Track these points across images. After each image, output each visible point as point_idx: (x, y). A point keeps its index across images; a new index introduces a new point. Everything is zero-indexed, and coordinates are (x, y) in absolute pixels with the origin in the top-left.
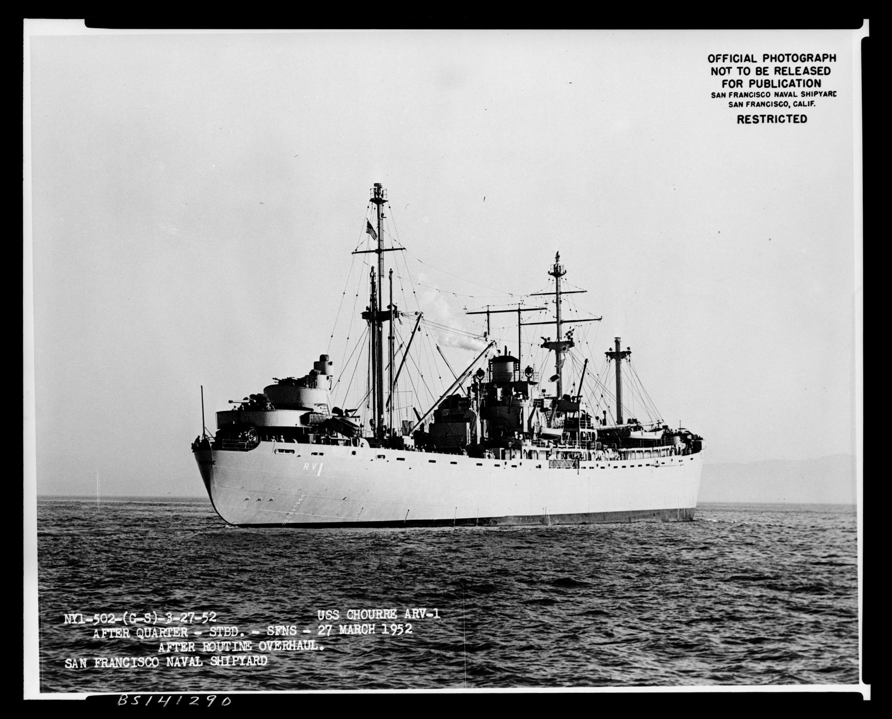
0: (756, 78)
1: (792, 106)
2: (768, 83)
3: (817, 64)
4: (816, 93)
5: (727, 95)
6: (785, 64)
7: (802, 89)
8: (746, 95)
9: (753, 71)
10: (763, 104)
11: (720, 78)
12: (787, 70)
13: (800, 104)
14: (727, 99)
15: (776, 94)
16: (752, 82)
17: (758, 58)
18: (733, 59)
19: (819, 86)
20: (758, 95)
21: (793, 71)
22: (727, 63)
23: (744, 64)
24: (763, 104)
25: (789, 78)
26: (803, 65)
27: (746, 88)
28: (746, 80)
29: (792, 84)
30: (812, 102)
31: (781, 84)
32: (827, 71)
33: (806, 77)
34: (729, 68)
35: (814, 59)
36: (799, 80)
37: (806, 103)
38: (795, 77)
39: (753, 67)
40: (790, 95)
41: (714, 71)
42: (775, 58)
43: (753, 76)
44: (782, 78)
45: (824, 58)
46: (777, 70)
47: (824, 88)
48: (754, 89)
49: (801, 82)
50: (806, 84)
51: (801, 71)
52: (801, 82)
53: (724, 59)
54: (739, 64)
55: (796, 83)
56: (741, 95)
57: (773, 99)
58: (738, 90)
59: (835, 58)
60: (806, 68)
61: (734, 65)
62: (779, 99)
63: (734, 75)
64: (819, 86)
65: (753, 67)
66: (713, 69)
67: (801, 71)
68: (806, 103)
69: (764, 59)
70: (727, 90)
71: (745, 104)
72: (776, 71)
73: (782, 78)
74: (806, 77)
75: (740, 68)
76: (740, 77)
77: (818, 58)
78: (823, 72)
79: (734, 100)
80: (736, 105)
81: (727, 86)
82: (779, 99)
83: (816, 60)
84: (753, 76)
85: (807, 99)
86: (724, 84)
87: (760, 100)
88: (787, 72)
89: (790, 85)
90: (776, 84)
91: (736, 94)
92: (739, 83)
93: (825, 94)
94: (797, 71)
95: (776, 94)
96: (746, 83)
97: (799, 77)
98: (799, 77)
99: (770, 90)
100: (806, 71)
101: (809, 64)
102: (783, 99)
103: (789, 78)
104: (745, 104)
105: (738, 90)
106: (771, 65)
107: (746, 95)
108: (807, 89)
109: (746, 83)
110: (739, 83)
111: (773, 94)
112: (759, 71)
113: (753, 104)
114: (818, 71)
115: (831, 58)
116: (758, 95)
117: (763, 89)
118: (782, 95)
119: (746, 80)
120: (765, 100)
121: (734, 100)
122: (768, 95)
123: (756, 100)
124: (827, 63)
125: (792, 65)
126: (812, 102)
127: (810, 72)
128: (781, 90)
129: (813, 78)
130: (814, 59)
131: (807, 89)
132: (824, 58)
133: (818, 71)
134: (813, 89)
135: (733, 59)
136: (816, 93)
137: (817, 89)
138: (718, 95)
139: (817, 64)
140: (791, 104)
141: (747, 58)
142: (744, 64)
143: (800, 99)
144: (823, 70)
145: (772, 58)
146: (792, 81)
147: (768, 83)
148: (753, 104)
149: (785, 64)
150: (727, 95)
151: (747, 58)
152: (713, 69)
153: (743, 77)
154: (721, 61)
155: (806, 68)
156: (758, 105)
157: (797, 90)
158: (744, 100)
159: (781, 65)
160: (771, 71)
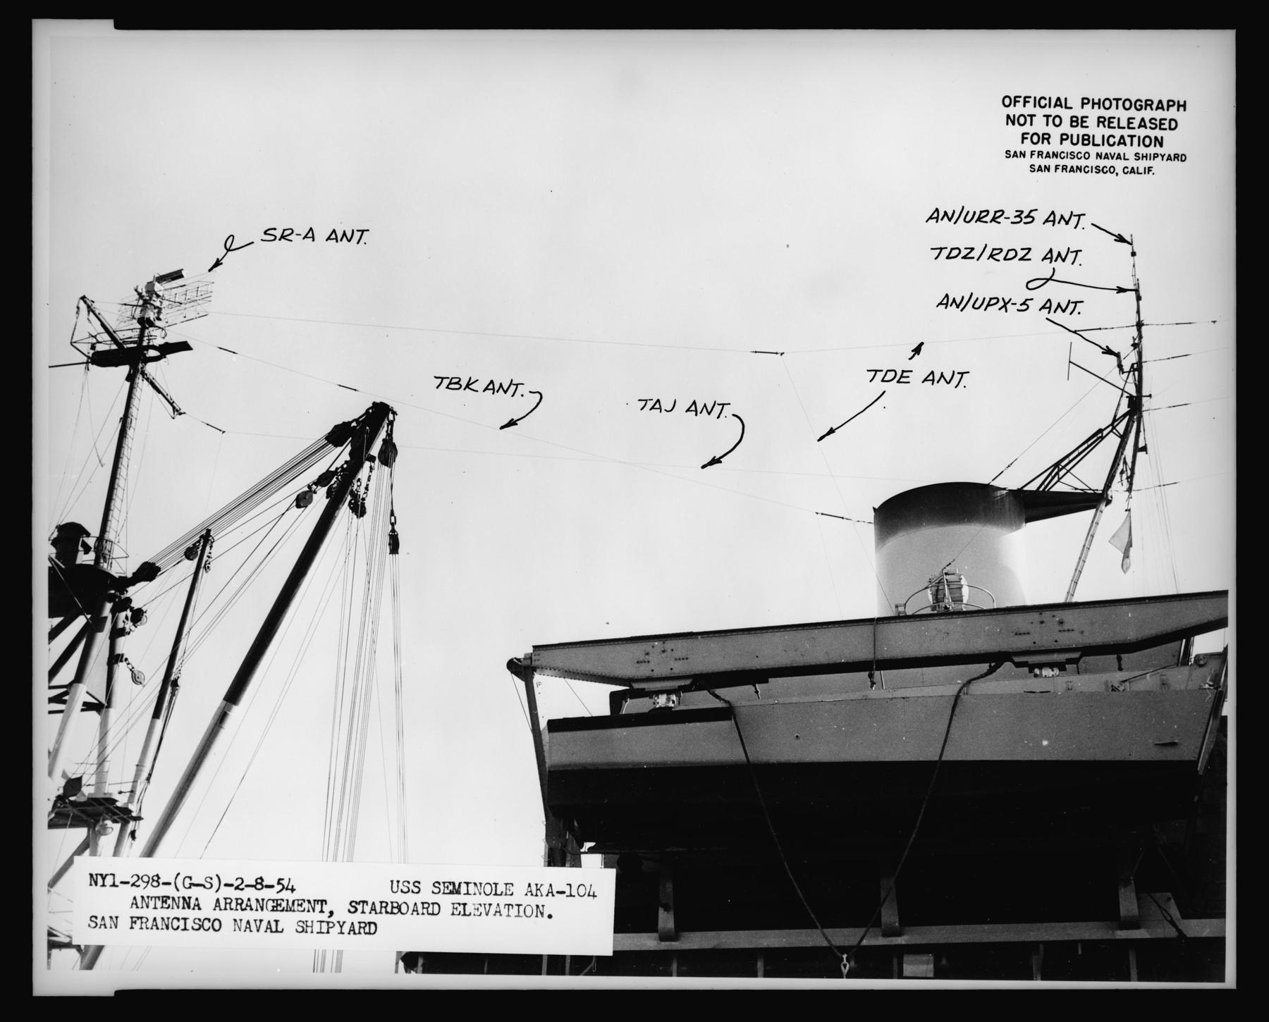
0: (1070, 131)
1: (1120, 172)
2: (1087, 140)
3: (1159, 114)
4: (1156, 156)
5: (1028, 154)
6: (1112, 112)
7: (1135, 149)
8: (1055, 155)
9: (1066, 121)
10: (1079, 169)
11: (1017, 130)
12: (1116, 121)
13: (1133, 171)
14: (1028, 161)
15: (1099, 156)
16: (1064, 138)
17: (1075, 102)
18: (1038, 102)
19: (1161, 145)
20: (1073, 155)
21: (1124, 123)
22: (1030, 109)
23: (1054, 111)
24: (1079, 169)
25: (1118, 133)
26: (1138, 115)
27: (1055, 146)
28: (1055, 133)
29: (1122, 141)
30: (1150, 169)
31: (1106, 140)
32: (1173, 124)
33: (1142, 132)
34: (1032, 116)
35: (1154, 106)
36: (1132, 137)
37: (1141, 170)
38: (1126, 132)
39: (1066, 115)
40: (1119, 157)
41: (1011, 120)
42: (1099, 104)
43: (1066, 128)
44: (1107, 132)
45: (1169, 106)
46: (1101, 121)
47: (1166, 150)
48: (1067, 147)
49: (1135, 140)
50: (1142, 142)
51: (1136, 123)
52: (1135, 140)
53: (1025, 102)
54: (1047, 111)
55: (1128, 140)
56: (1048, 155)
57: (1093, 162)
58: (1044, 147)
59: (1184, 106)
60: (1143, 120)
61: (1039, 112)
62: (1102, 163)
63: (1039, 126)
64: (1161, 145)
65: (1066, 115)
66: (1008, 116)
67: (1136, 123)
68: (1141, 170)
69: (1083, 104)
70: (1028, 147)
71: (1053, 169)
72: (1099, 122)
73: (1107, 132)
74: (1142, 132)
75: (1047, 116)
76: (1047, 130)
77: (1160, 106)
78: (1166, 126)
79: (1038, 162)
80: (1040, 169)
81: (1027, 142)
82: (1102, 163)
83: (1157, 108)
84: (1066, 128)
85: (1142, 164)
86: (1023, 138)
87: (1075, 163)
88: (1115, 124)
89: (1119, 143)
90: (1098, 140)
91: (1040, 154)
92: (1046, 138)
93: (1169, 158)
94: (1129, 123)
95: (1099, 156)
96: (1055, 138)
97: (1131, 132)
98: (1131, 132)
99: (1090, 148)
100: (1142, 124)
101: (1147, 114)
102: (1108, 163)
103: (1118, 133)
104: (1053, 169)
105: (1044, 147)
106: (1093, 114)
107: (1055, 155)
108: (1142, 150)
109: (1055, 138)
110: (1046, 138)
111: (1093, 155)
112: (1075, 121)
113: (1064, 168)
114: (1159, 124)
115: (1179, 106)
116: (1073, 155)
117: (1080, 148)
118: (1106, 157)
119: (1055, 133)
120: (1082, 163)
121: (1038, 162)
122: (1087, 156)
123: (1069, 162)
124: (1173, 113)
125: (1123, 115)
126: (1150, 169)
127: (1148, 125)
128: (1105, 149)
129: (1153, 134)
130: (1154, 106)
131: (1142, 150)
132: (1169, 106)
133: (1159, 124)
134: (1152, 150)
135: (1038, 102)
136: (1156, 156)
137: (1158, 150)
138: (1015, 155)
139: (1159, 114)
140: (1119, 170)
141: (1058, 103)
142: (1054, 111)
143: (1133, 163)
144: (1167, 122)
145: (1094, 104)
146: (1122, 137)
147: (1087, 140)
148: (1064, 168)
149: (1112, 112)
150: (1028, 154)
151: (1058, 103)
152: (1008, 116)
153: (1051, 129)
154: (1020, 105)
155: (1143, 120)
156: (1072, 170)
157: (1129, 151)
158: (1052, 162)
159: (1107, 114)
160: (1092, 122)
